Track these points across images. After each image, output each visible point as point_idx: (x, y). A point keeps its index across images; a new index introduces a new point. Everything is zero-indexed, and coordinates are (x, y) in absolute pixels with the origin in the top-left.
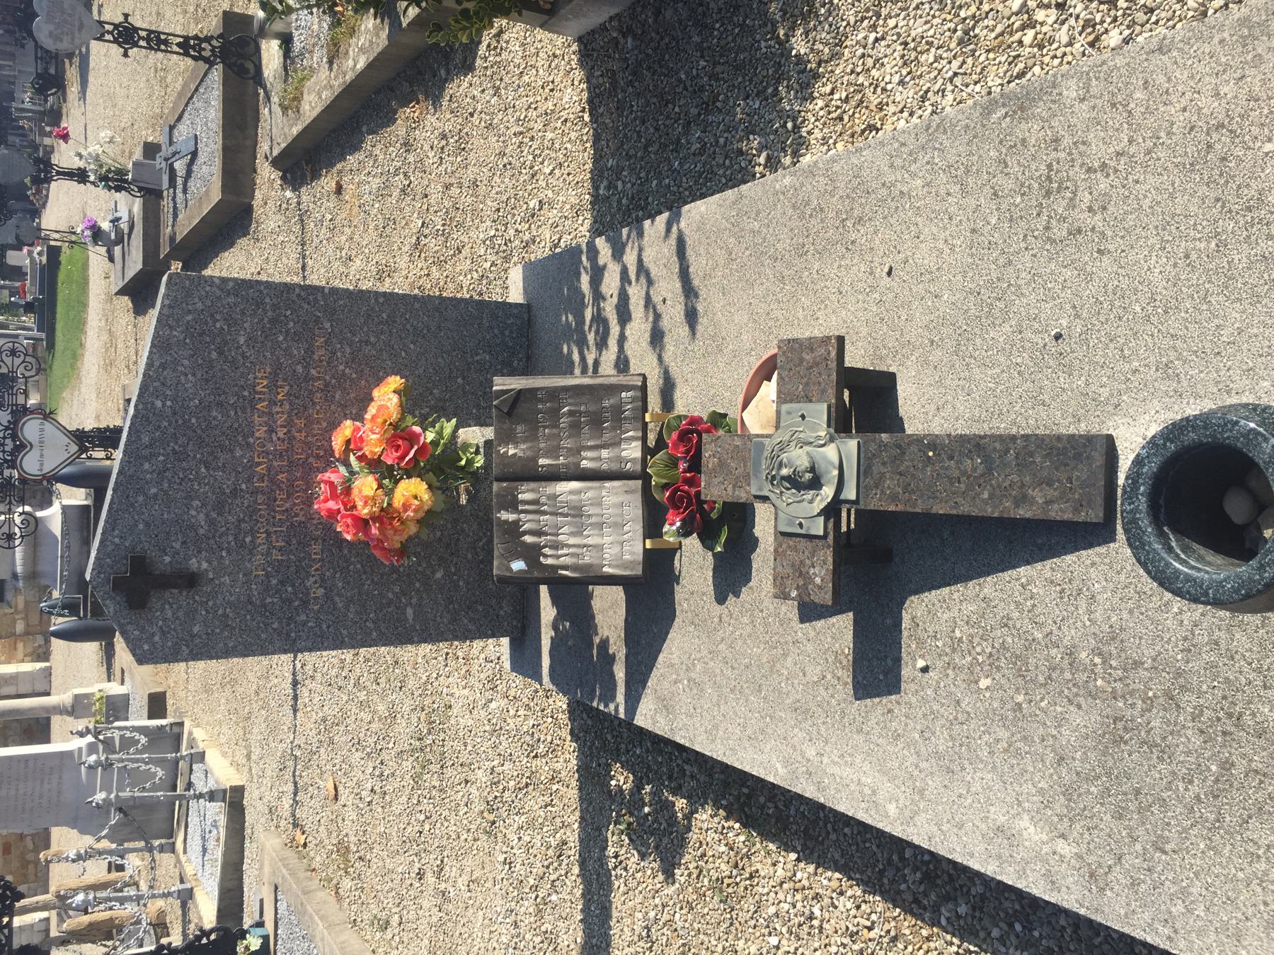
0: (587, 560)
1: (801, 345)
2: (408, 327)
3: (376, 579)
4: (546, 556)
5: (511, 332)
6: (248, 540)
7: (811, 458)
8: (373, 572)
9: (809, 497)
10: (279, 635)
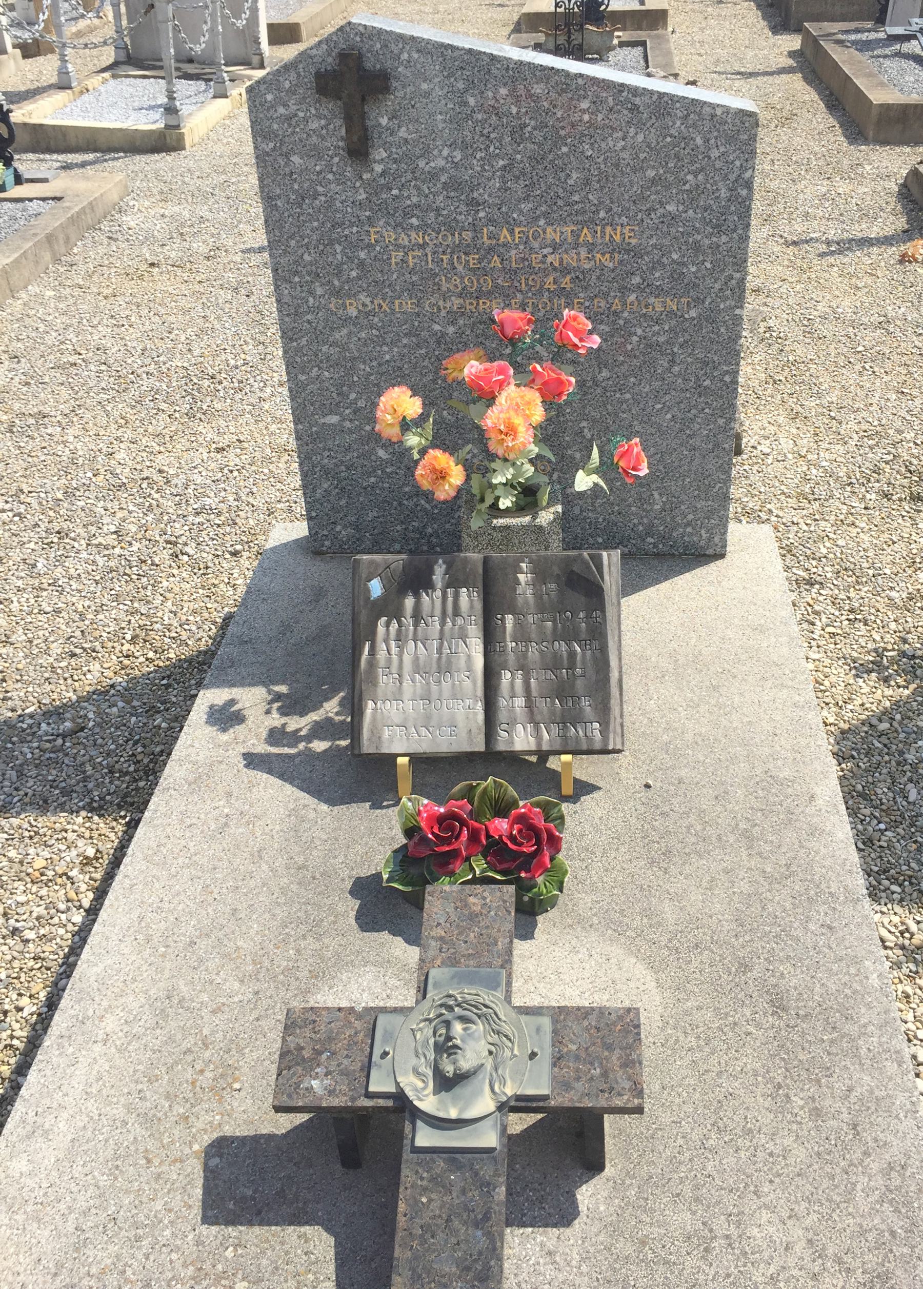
0: (382, 680)
1: (630, 1047)
2: (694, 411)
3: (372, 378)
4: (388, 625)
5: (690, 535)
6: (414, 221)
7: (475, 1072)
8: (382, 374)
9: (422, 1069)
10: (295, 262)
